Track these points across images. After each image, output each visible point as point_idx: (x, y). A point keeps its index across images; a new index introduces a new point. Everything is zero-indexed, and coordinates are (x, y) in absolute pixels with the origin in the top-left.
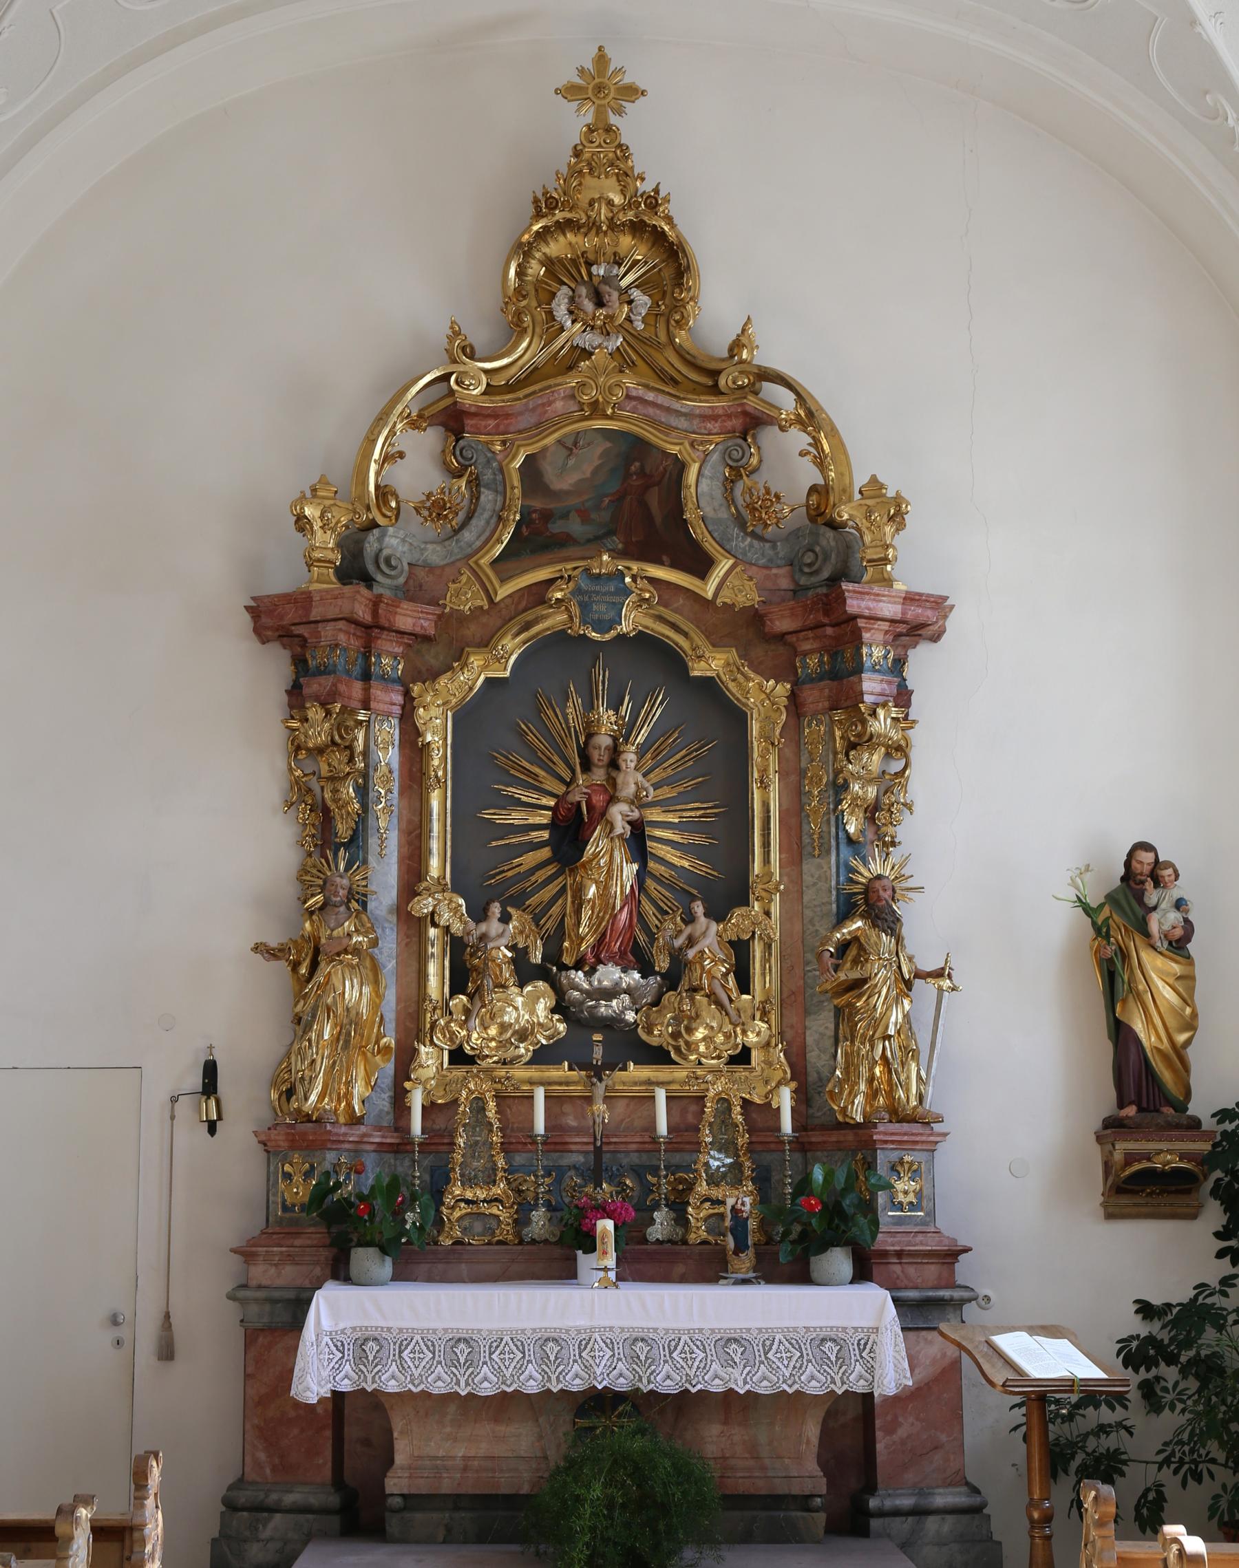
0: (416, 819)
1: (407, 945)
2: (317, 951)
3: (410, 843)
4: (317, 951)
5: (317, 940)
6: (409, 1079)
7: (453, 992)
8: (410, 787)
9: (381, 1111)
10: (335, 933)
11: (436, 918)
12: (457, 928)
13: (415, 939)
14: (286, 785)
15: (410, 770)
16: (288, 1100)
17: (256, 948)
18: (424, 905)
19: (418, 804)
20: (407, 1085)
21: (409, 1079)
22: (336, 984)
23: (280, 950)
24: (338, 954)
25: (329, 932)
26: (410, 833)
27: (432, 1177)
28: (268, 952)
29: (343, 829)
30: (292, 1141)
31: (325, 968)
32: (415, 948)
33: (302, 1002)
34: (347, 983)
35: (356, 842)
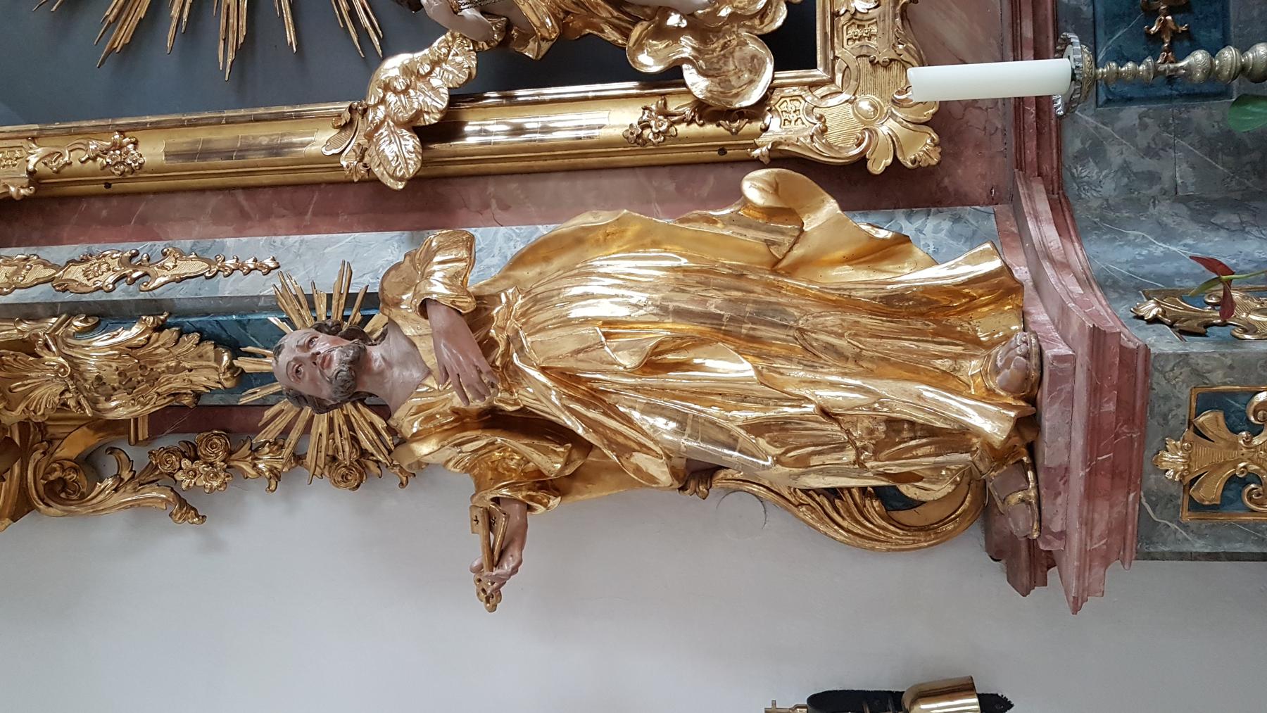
0: (213, 201)
1: (505, 207)
2: (493, 419)
3: (266, 215)
4: (493, 419)
5: (462, 420)
6: (862, 161)
7: (625, 71)
8: (143, 221)
9: (951, 234)
10: (431, 361)
11: (431, 119)
12: (454, 62)
13: (492, 187)
14: (56, 509)
15: (105, 223)
16: (912, 504)
17: (492, 599)
18: (398, 155)
19: (180, 200)
20: (878, 166)
21: (862, 161)
22: (571, 345)
23: (491, 527)
24: (488, 346)
25: (431, 382)
26: (244, 216)
27: (1129, 100)
28: (495, 562)
29: (206, 372)
30: (1115, 473)
31: (539, 394)
32: (513, 186)
33: (639, 459)
34: (577, 312)
35: (231, 330)
